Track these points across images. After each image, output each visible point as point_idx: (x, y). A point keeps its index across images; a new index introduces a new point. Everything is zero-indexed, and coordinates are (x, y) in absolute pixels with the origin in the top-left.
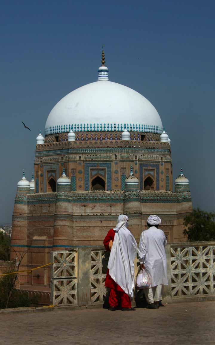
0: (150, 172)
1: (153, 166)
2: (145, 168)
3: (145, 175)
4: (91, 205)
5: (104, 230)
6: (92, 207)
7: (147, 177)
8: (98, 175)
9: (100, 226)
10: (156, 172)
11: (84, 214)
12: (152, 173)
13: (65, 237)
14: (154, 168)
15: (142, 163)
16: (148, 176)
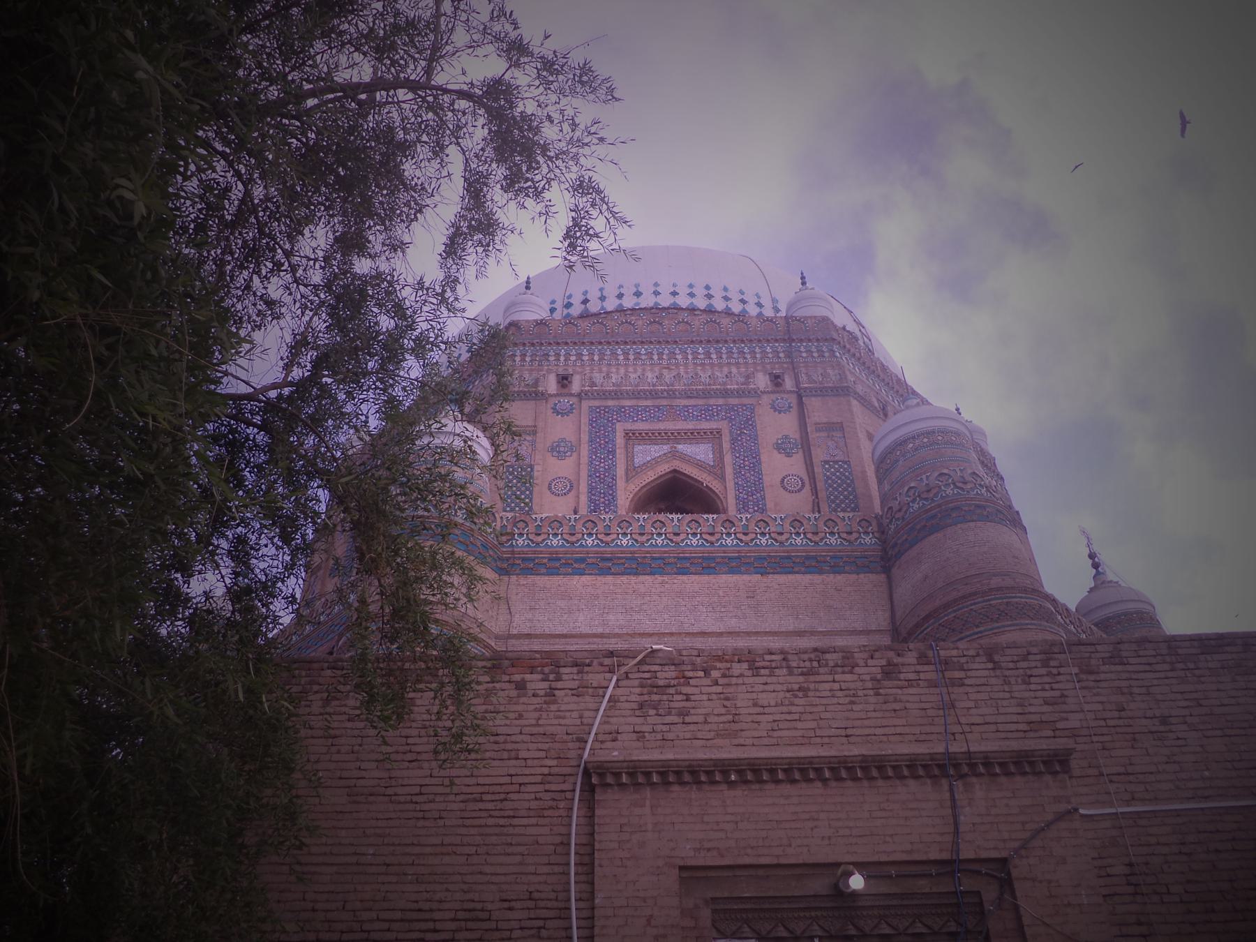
0: (680, 447)
1: (707, 413)
2: (629, 426)
3: (638, 461)
7: (650, 476)
10: (726, 445)
12: (702, 452)
14: (713, 425)
15: (610, 403)
16: (664, 468)
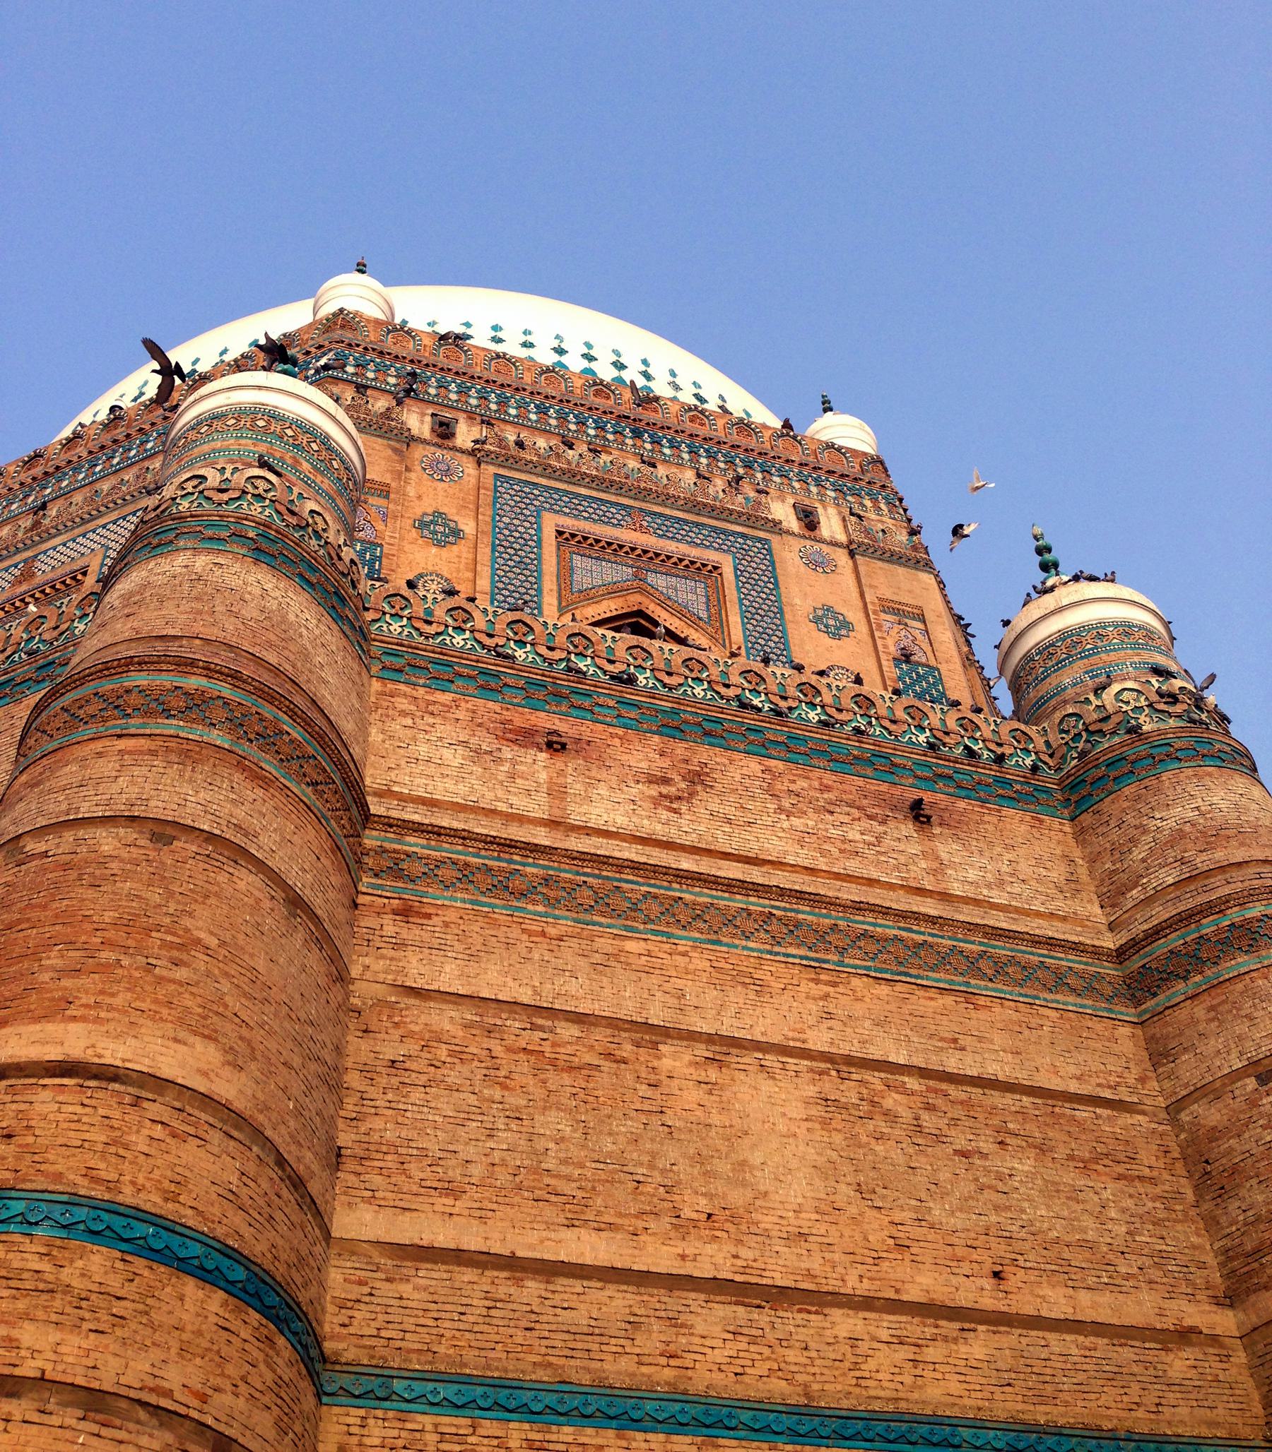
4: (644, 754)
5: (891, 1116)
6: (666, 781)
8: (637, 598)
9: (819, 1040)
11: (542, 831)
13: (209, 1054)
